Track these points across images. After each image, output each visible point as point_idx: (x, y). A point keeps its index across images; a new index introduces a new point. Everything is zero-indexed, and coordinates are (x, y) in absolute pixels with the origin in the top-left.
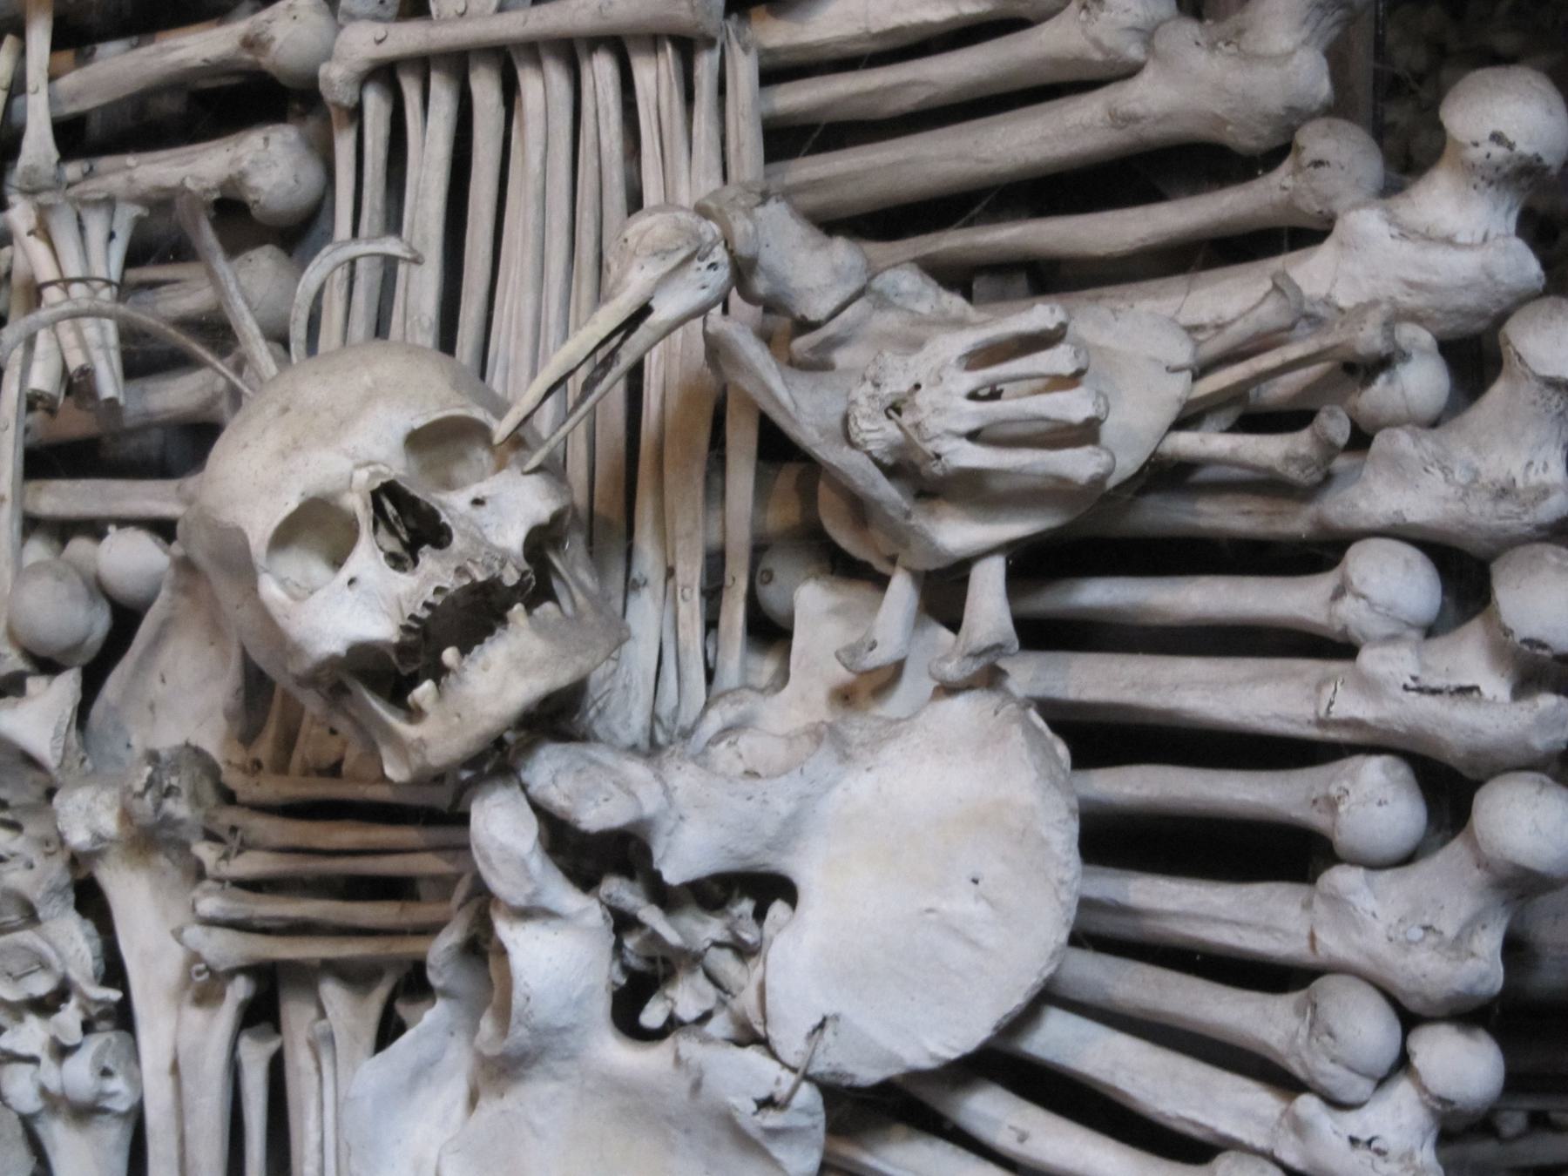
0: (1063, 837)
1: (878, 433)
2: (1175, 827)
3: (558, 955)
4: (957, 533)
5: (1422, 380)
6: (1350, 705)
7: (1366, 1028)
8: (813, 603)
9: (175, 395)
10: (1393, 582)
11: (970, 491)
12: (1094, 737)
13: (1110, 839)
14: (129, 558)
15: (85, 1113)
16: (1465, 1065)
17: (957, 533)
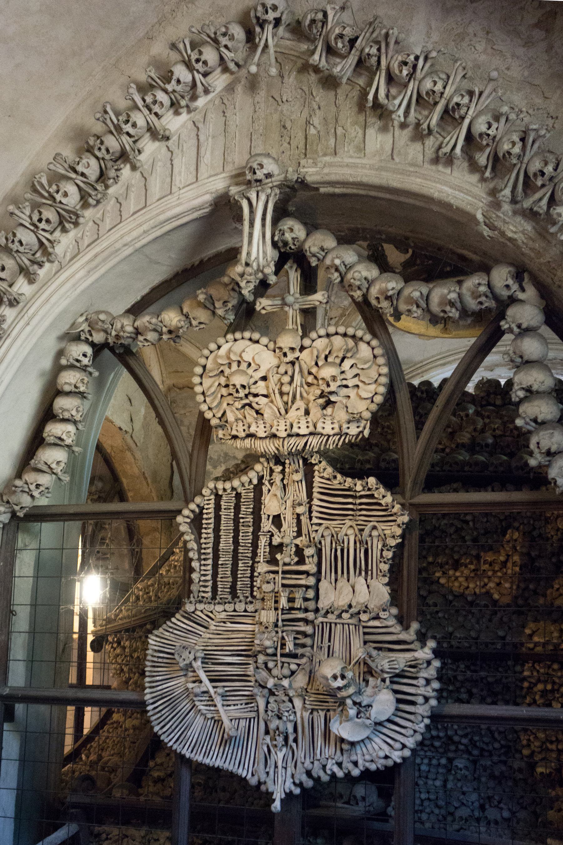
0: (395, 701)
1: (380, 668)
2: (403, 700)
3: (352, 712)
4: (386, 675)
5: (425, 665)
6: (419, 692)
7: (420, 718)
8: (371, 679)
9: (300, 651)
10: (422, 682)
11: (388, 673)
12: (396, 692)
13: (399, 701)
14: (293, 667)
15: (290, 721)
16: (427, 721)
17: (386, 675)
